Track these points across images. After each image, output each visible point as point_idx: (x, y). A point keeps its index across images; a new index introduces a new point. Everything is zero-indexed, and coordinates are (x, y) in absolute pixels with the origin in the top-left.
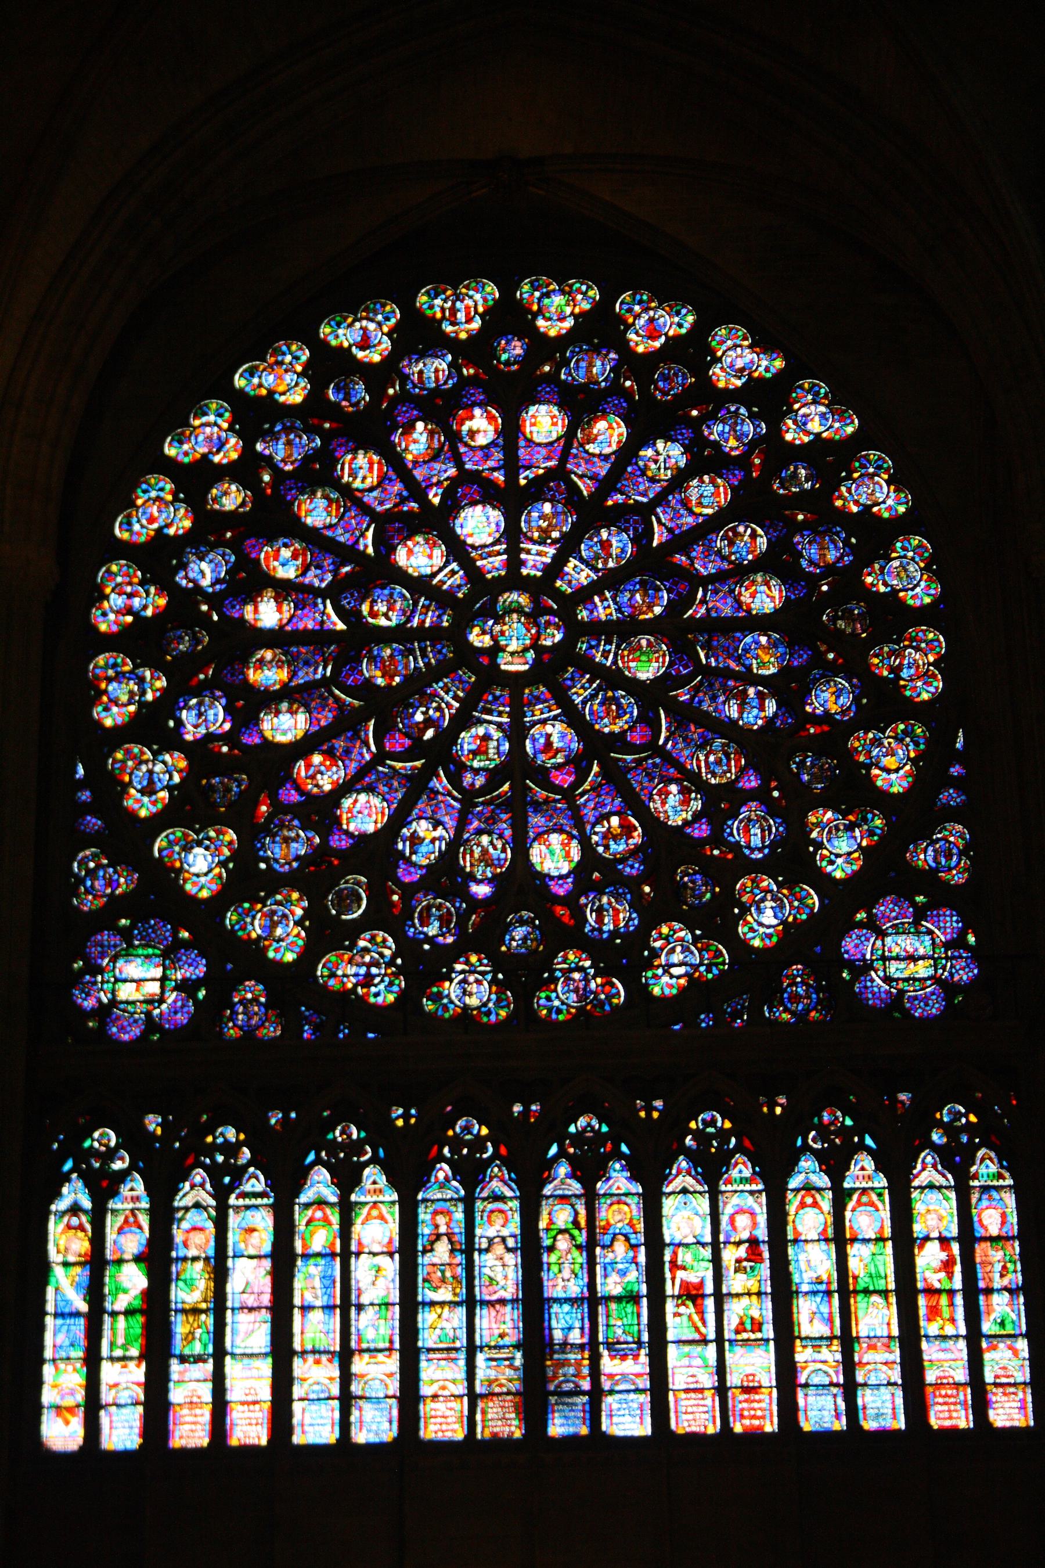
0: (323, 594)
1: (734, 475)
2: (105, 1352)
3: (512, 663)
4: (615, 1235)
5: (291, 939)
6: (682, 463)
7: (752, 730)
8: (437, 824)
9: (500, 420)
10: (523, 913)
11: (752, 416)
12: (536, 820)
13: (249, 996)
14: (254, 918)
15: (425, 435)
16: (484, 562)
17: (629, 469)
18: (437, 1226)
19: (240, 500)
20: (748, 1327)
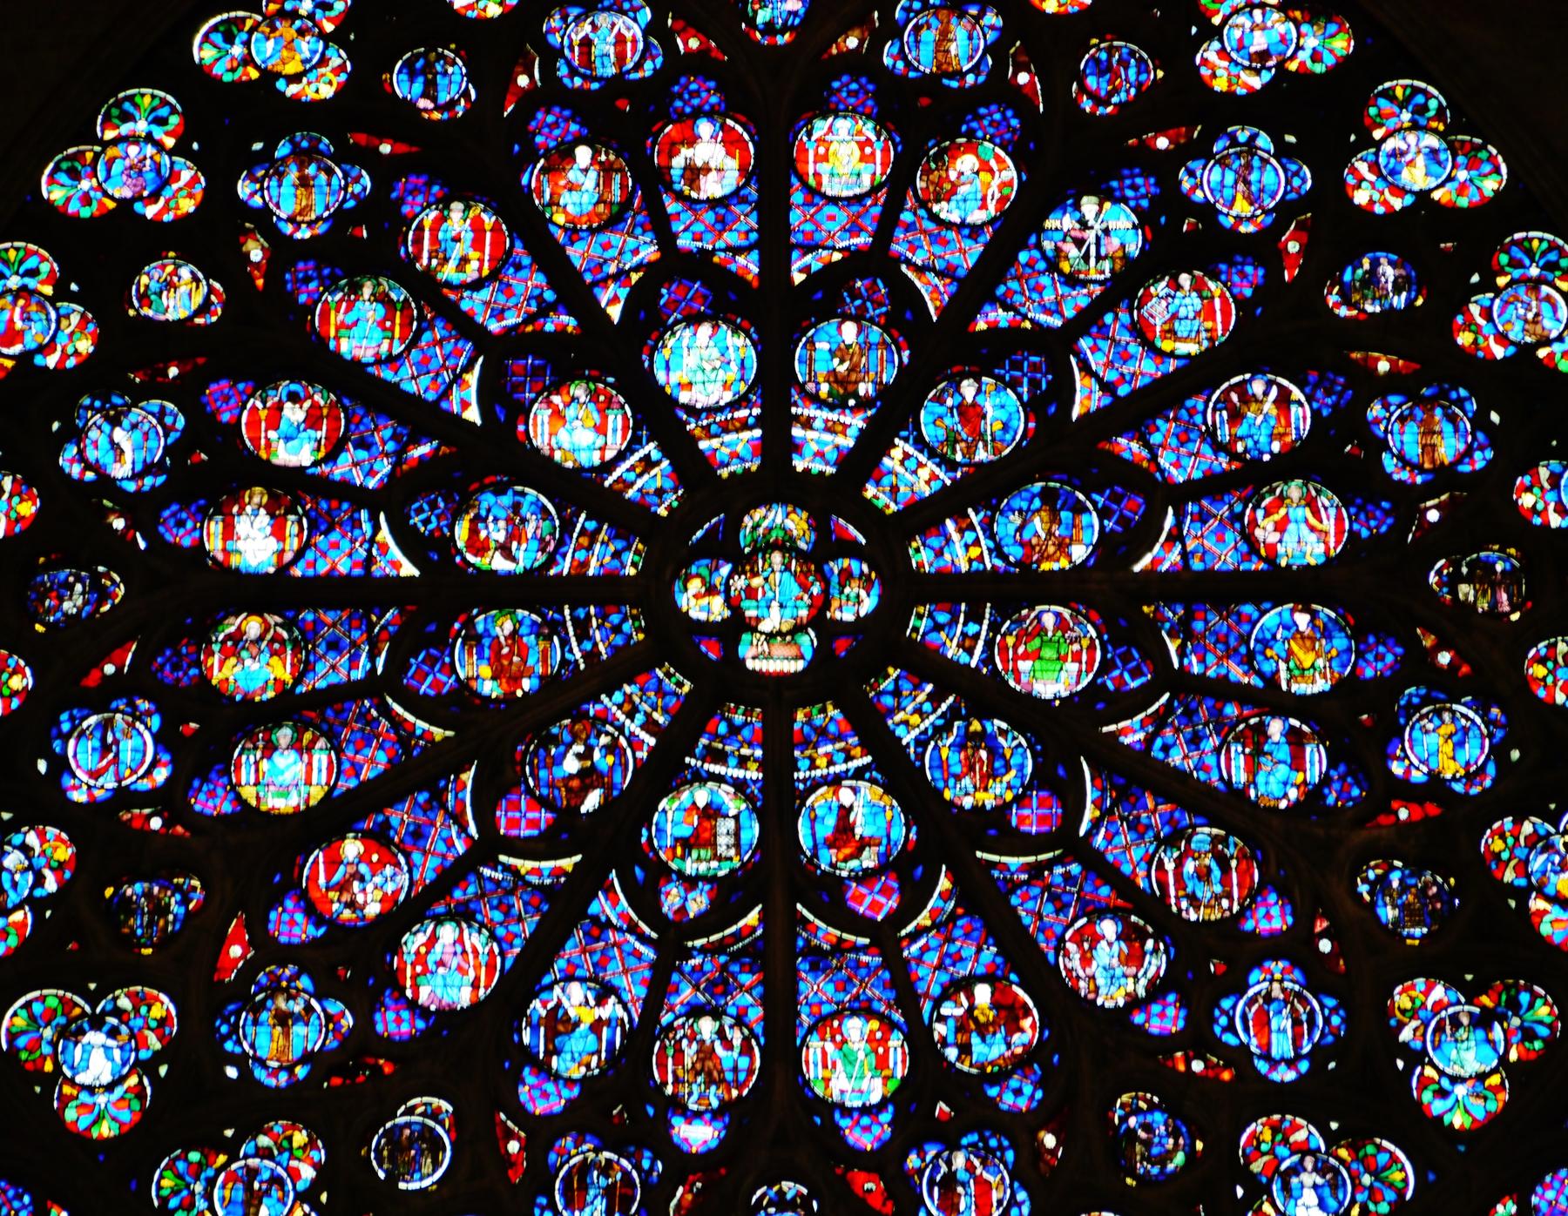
0: (372, 501)
1: (1243, 275)
3: (769, 657)
6: (1134, 249)
7: (1276, 809)
8: (605, 991)
10: (786, 1185)
11: (1282, 152)
12: (816, 989)
14: (211, 1183)
15: (593, 174)
16: (715, 443)
17: (1023, 257)
19: (198, 299)
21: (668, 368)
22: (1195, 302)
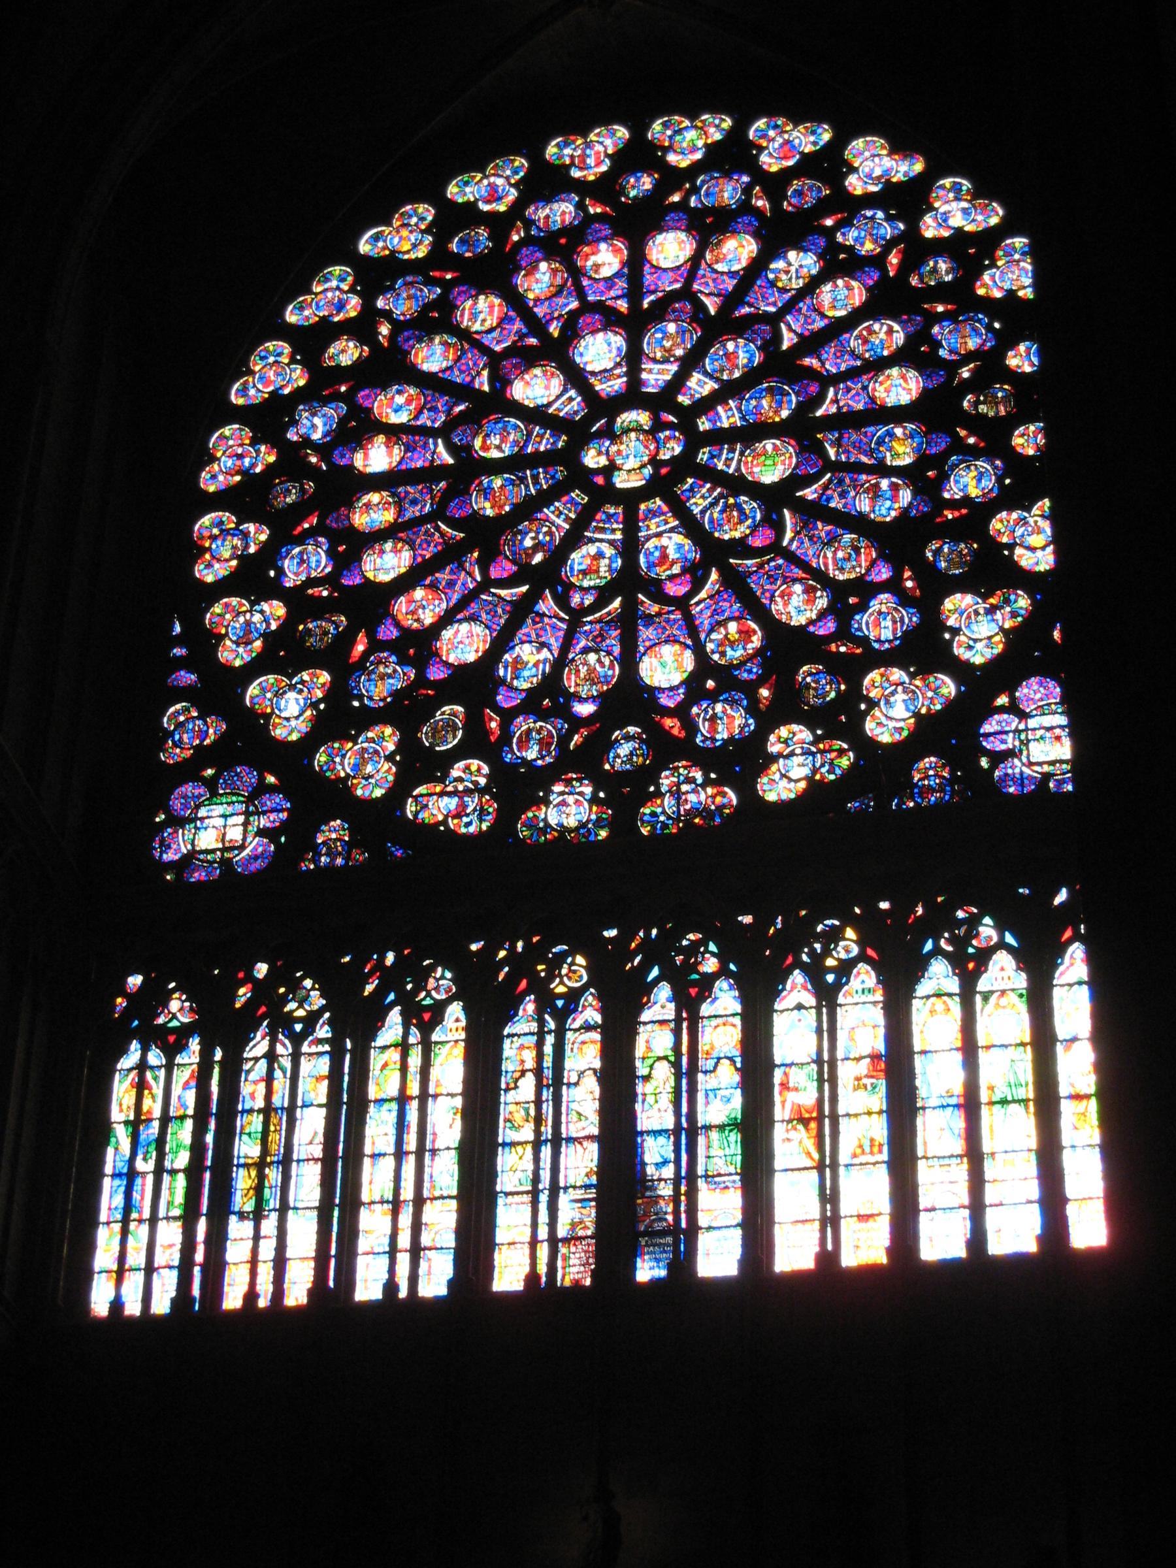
2: (162, 1213)
4: (719, 1059)
5: (381, 775)
7: (885, 522)
8: (543, 645)
9: (625, 252)
11: (889, 218)
12: (647, 634)
13: (334, 836)
14: (344, 756)
15: (548, 275)
16: (604, 386)
18: (522, 1062)
19: (356, 355)
20: (867, 1149)
21: (581, 355)
22: (842, 293)
